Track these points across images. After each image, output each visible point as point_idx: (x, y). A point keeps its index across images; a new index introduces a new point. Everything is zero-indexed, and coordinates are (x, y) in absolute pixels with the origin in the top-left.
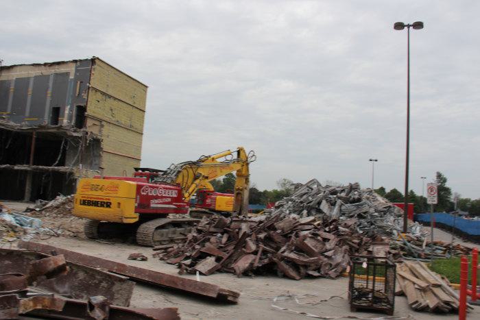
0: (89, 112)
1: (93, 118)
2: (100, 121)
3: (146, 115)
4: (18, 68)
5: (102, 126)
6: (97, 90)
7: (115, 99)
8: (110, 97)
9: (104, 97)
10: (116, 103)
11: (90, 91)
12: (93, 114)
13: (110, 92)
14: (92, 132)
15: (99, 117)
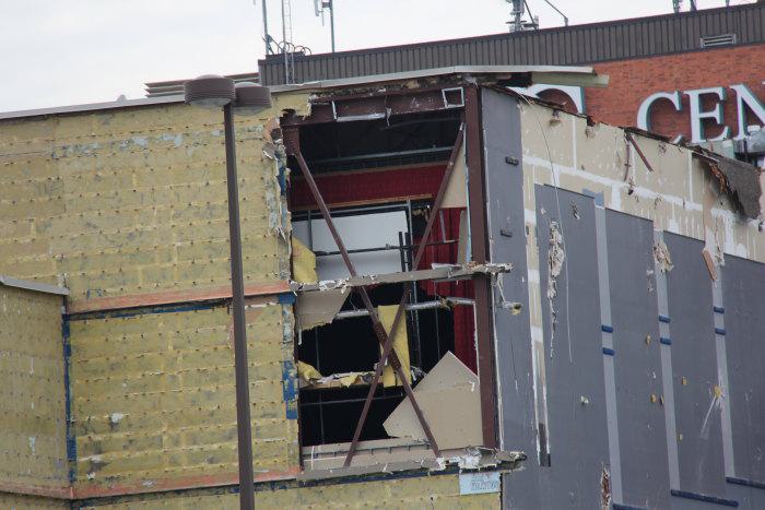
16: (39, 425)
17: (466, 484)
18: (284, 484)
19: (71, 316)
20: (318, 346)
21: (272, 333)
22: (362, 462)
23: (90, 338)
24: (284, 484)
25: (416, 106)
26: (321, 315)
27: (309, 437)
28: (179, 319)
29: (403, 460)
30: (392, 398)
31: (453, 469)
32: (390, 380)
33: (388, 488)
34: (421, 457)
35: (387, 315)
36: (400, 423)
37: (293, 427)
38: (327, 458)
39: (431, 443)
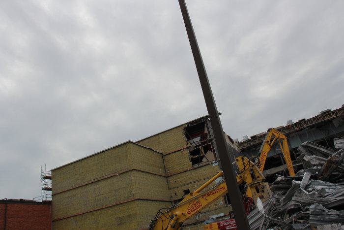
16: (161, 168)
17: (214, 165)
18: (191, 170)
19: (163, 156)
20: (192, 153)
21: (187, 152)
22: (200, 165)
23: (166, 158)
24: (191, 170)
25: (199, 122)
26: (192, 149)
27: (193, 164)
28: (176, 154)
29: (203, 164)
30: (202, 157)
31: (212, 163)
32: (202, 155)
33: (204, 168)
34: (207, 163)
35: (200, 147)
36: (204, 160)
37: (191, 163)
38: (196, 166)
39: (208, 161)
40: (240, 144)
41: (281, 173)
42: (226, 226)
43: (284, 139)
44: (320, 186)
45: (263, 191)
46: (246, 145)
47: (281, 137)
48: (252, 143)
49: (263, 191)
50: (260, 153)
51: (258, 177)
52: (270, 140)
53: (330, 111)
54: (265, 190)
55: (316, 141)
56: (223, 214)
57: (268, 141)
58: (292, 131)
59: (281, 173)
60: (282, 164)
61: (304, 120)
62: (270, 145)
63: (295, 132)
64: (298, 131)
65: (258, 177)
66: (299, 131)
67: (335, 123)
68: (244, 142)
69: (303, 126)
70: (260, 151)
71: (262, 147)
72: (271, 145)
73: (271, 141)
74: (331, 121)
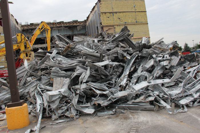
0: (103, 24)
1: (107, 26)
2: (113, 26)
3: (148, 13)
4: (90, 16)
5: (115, 28)
6: (105, 13)
7: (120, 12)
8: (116, 13)
9: (112, 14)
10: (121, 14)
11: (101, 15)
12: (106, 24)
13: (115, 10)
14: (108, 33)
15: (111, 24)
17: (2, 35)
40: (22, 26)
41: (43, 48)
42: (4, 73)
43: (49, 30)
44: (60, 58)
45: (30, 56)
46: (26, 28)
47: (47, 28)
48: (30, 27)
49: (30, 56)
50: (33, 34)
51: (29, 48)
52: (41, 28)
53: (78, 21)
54: (31, 56)
55: (66, 35)
56: (3, 67)
57: (40, 29)
58: (55, 26)
59: (43, 48)
60: (45, 44)
61: (63, 22)
62: (40, 31)
63: (56, 27)
64: (58, 27)
65: (29, 48)
66: (58, 27)
67: (78, 28)
68: (25, 26)
69: (61, 25)
70: (33, 33)
71: (35, 31)
72: (41, 31)
73: (42, 28)
74: (76, 26)
